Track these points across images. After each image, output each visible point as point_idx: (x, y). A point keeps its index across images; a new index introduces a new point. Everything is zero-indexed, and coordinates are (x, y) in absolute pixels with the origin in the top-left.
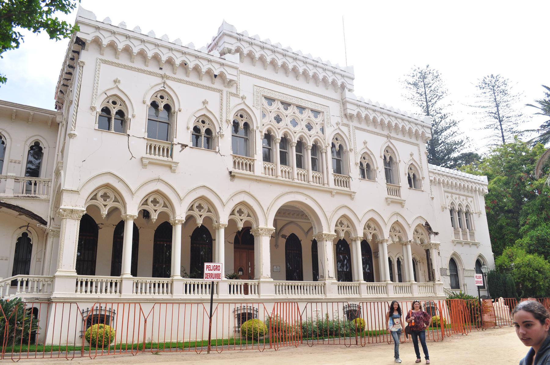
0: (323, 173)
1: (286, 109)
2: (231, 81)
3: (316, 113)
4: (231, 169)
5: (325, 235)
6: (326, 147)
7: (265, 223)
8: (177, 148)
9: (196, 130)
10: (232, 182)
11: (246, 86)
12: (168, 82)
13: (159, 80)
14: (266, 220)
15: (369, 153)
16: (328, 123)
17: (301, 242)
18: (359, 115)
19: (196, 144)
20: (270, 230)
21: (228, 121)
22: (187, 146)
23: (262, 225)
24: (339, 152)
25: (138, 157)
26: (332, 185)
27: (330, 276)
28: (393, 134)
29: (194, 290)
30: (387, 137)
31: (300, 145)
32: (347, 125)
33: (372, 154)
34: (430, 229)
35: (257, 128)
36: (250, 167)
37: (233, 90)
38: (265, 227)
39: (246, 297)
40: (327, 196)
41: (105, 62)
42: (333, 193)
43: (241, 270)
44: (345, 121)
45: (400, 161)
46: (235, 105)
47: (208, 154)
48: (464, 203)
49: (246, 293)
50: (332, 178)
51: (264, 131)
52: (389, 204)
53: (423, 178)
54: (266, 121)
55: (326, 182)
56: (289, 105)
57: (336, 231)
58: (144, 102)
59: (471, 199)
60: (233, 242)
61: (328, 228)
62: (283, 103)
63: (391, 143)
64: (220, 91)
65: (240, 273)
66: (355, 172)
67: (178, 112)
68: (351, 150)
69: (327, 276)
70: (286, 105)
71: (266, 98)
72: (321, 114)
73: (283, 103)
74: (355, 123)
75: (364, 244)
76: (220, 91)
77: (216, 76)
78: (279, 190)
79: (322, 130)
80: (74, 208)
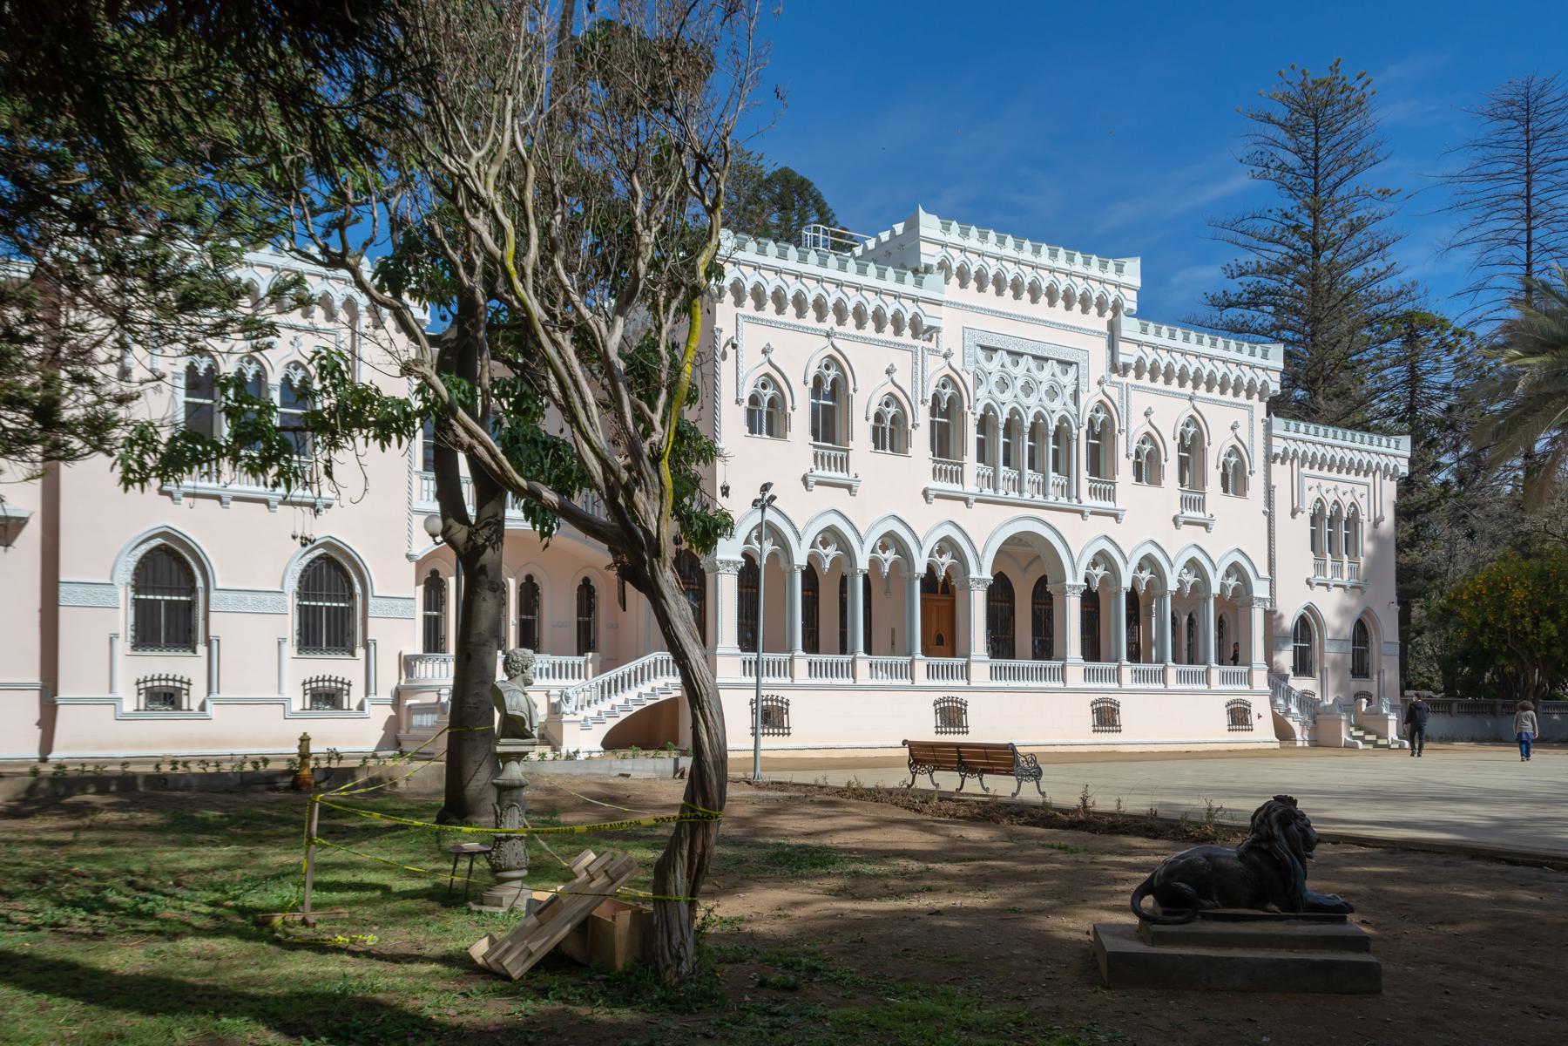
0: (1068, 475)
2: (930, 328)
7: (981, 572)
9: (879, 417)
11: (951, 326)
20: (984, 581)
23: (974, 574)
24: (1102, 435)
30: (1191, 399)
31: (1037, 430)
36: (958, 477)
46: (935, 369)
48: (1347, 500)
50: (1085, 485)
51: (980, 411)
54: (982, 392)
57: (1087, 580)
59: (1364, 489)
66: (1125, 467)
71: (983, 347)
79: (1076, 396)
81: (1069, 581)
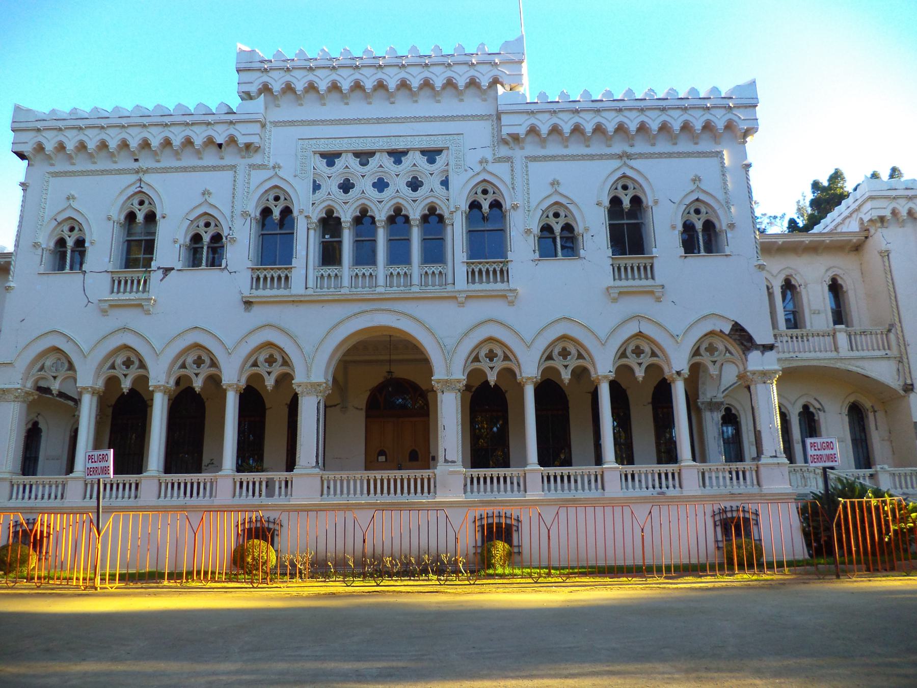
1: (363, 164)
2: (248, 146)
3: (431, 155)
4: (246, 292)
5: (438, 381)
6: (452, 213)
7: (312, 371)
8: (156, 276)
10: (247, 314)
12: (146, 178)
13: (134, 178)
14: (308, 370)
15: (564, 201)
16: (458, 166)
17: (507, 395)
18: (533, 131)
19: (194, 260)
21: (245, 214)
22: (173, 269)
25: (95, 301)
26: (461, 282)
27: (449, 458)
28: (641, 147)
29: (198, 493)
32: (508, 159)
33: (572, 203)
34: (750, 339)
35: (301, 212)
37: (257, 159)
38: (305, 381)
39: (270, 501)
40: (448, 308)
41: (56, 174)
42: (459, 300)
43: (382, 453)
44: (504, 151)
45: (656, 202)
47: (214, 273)
49: (270, 494)
50: (461, 271)
52: (615, 300)
53: (732, 226)
55: (450, 280)
56: (372, 154)
58: (109, 219)
60: (364, 407)
61: (449, 370)
62: (357, 154)
63: (632, 168)
64: (233, 167)
65: (382, 458)
67: (162, 220)
68: (515, 207)
69: (441, 459)
70: (364, 156)
71: (323, 155)
72: (445, 152)
73: (357, 154)
74: (531, 149)
75: (614, 386)
76: (233, 167)
77: (220, 146)
78: (338, 312)
79: (445, 183)
80: (7, 386)
81: (439, 374)
